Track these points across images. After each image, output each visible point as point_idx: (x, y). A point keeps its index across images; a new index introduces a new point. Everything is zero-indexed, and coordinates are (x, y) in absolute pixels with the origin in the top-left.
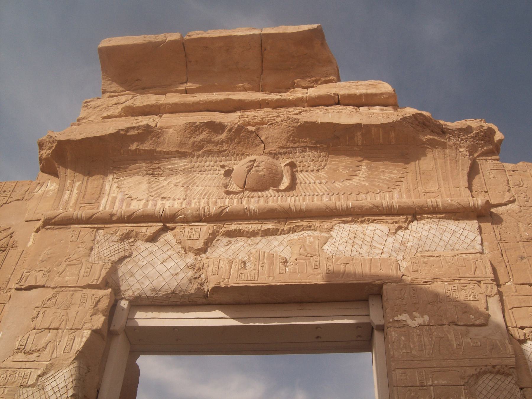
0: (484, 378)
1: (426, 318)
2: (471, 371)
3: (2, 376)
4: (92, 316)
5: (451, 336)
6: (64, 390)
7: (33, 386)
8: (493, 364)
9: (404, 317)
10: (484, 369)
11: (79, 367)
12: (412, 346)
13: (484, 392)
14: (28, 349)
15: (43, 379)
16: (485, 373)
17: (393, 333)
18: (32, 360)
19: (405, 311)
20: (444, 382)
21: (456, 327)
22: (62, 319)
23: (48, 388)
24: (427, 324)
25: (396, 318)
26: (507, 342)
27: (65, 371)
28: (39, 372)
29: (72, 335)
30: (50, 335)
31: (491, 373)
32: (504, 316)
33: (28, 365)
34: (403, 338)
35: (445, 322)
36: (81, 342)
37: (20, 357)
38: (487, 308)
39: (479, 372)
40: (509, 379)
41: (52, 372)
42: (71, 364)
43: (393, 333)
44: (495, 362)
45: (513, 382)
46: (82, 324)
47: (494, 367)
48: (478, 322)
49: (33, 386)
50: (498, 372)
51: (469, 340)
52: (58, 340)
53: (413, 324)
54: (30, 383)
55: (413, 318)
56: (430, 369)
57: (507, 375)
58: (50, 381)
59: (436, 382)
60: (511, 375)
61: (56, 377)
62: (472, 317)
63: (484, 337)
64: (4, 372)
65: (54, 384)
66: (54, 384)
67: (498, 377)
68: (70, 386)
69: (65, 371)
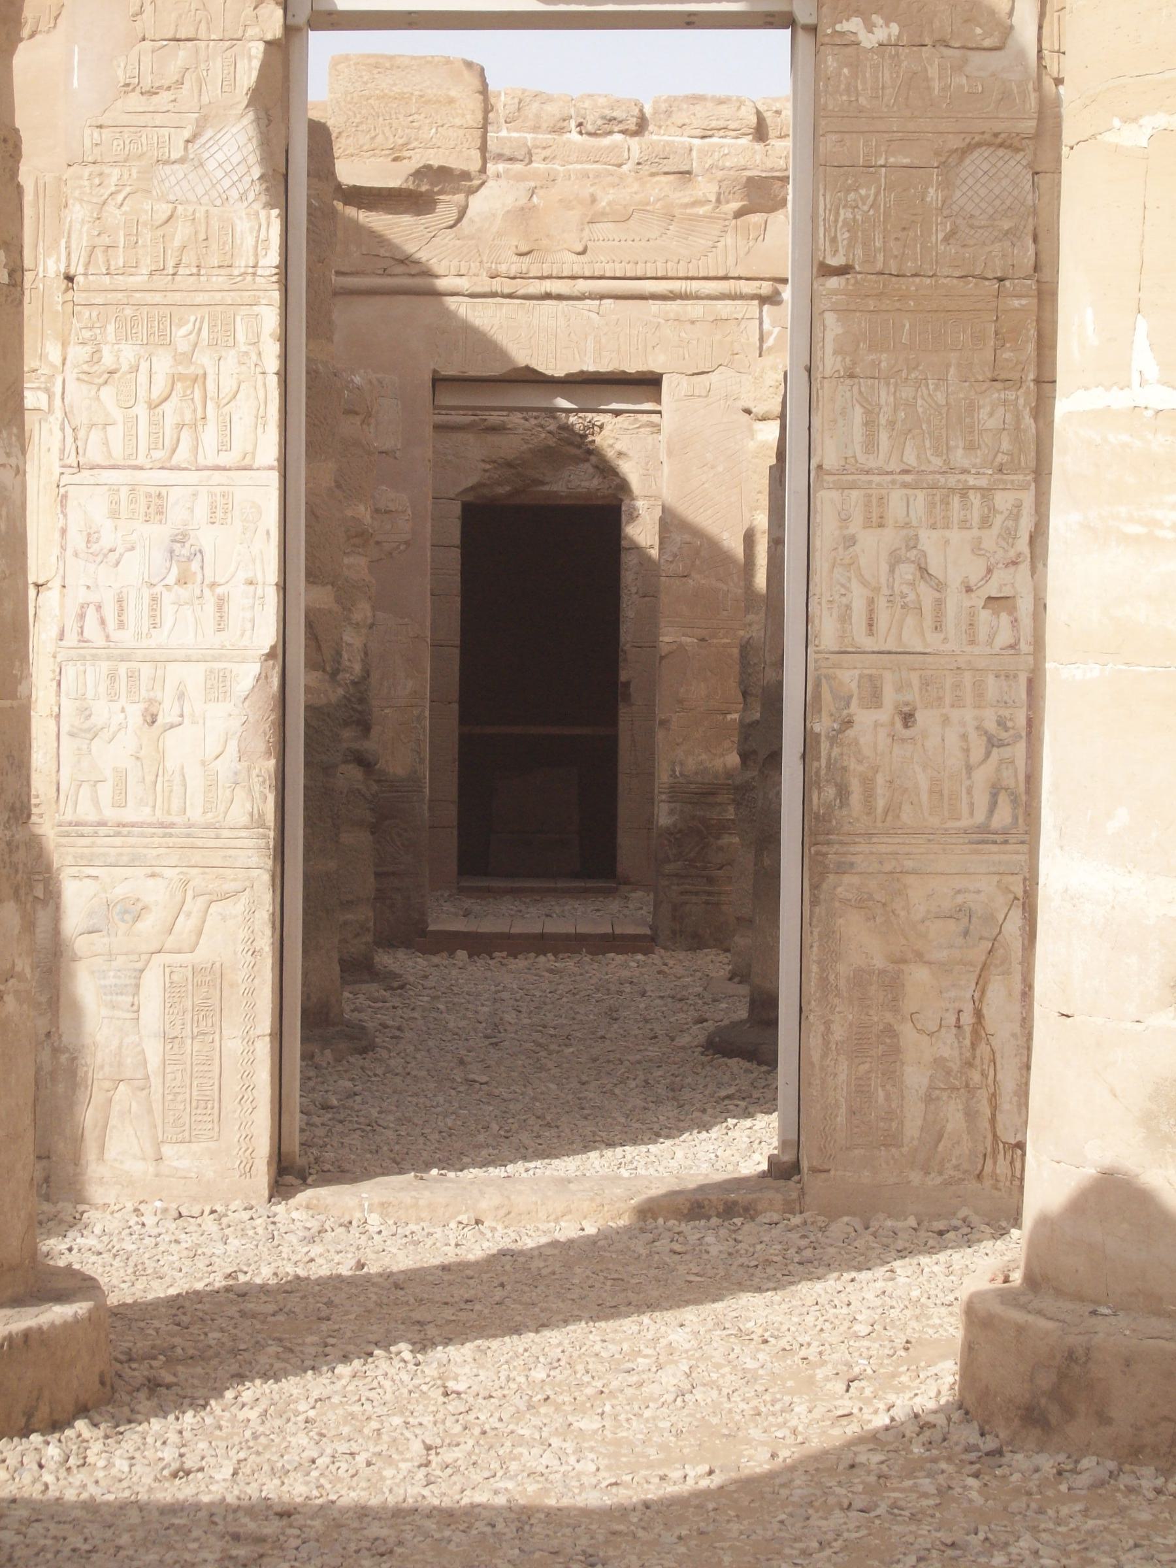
0: (976, 154)
1: (895, 28)
2: (955, 143)
3: (115, 143)
4: (255, 8)
5: (933, 72)
6: (242, 169)
7: (182, 160)
8: (997, 130)
9: (854, 25)
10: (977, 138)
11: (258, 119)
12: (860, 87)
13: (970, 181)
14: (146, 84)
15: (196, 146)
16: (979, 145)
17: (830, 58)
18: (165, 109)
19: (858, 12)
20: (906, 161)
21: (948, 52)
22: (198, 19)
23: (211, 165)
24: (893, 42)
25: (838, 27)
26: (1031, 86)
27: (234, 130)
28: (187, 134)
29: (229, 53)
30: (183, 53)
31: (990, 145)
32: (1040, 27)
33: (159, 119)
34: (845, 71)
35: (927, 41)
36: (250, 69)
37: (135, 101)
38: (1011, 14)
39: (969, 144)
40: (1019, 156)
41: (209, 133)
42: (242, 116)
43: (830, 58)
44: (999, 126)
45: (1024, 162)
46: (241, 29)
47: (996, 135)
48: (987, 43)
49: (182, 160)
50: (1001, 145)
51: (964, 81)
52: (203, 66)
53: (868, 40)
54: (175, 156)
55: (870, 27)
56: (886, 136)
57: (1017, 150)
58: (212, 150)
59: (892, 160)
60: (1023, 150)
61: (221, 143)
62: (979, 31)
63: (993, 75)
64: (118, 135)
65: (220, 157)
66: (220, 157)
67: (1001, 152)
68: (253, 159)
69: (234, 130)
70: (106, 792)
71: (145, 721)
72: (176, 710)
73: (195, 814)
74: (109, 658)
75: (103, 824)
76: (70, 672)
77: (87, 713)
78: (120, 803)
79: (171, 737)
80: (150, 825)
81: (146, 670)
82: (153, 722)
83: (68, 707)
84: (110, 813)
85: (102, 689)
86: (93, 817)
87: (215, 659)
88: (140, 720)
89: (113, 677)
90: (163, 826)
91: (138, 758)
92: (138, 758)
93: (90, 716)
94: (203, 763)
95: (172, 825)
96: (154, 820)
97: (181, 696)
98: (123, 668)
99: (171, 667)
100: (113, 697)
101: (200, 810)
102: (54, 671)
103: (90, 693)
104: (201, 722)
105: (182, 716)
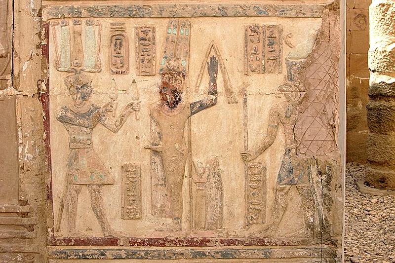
70: (112, 199)
71: (164, 99)
72: (205, 85)
73: (236, 228)
74: (112, 14)
75: (113, 241)
76: (60, 35)
77: (85, 90)
78: (131, 213)
79: (200, 123)
80: (178, 242)
81: (161, 29)
82: (176, 102)
83: (57, 81)
84: (119, 227)
85: (104, 58)
86: (97, 233)
87: (260, 12)
88: (157, 99)
89: (118, 40)
90: (191, 243)
91: (156, 152)
92: (156, 152)
93: (89, 95)
94: (244, 157)
95: (204, 242)
96: (181, 235)
97: (213, 66)
98: (131, 27)
99: (198, 25)
100: (120, 69)
101: (242, 222)
102: (40, 34)
103: (88, 63)
104: (241, 100)
105: (214, 92)
